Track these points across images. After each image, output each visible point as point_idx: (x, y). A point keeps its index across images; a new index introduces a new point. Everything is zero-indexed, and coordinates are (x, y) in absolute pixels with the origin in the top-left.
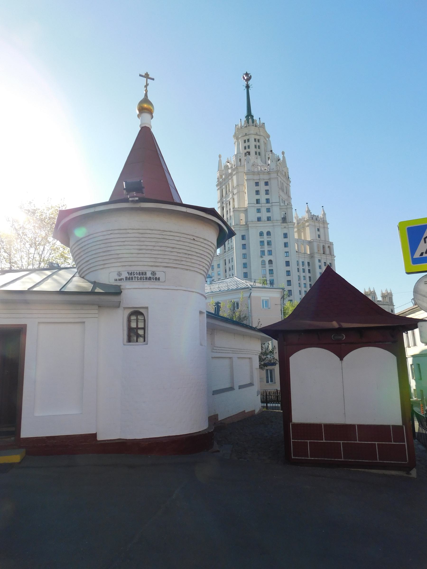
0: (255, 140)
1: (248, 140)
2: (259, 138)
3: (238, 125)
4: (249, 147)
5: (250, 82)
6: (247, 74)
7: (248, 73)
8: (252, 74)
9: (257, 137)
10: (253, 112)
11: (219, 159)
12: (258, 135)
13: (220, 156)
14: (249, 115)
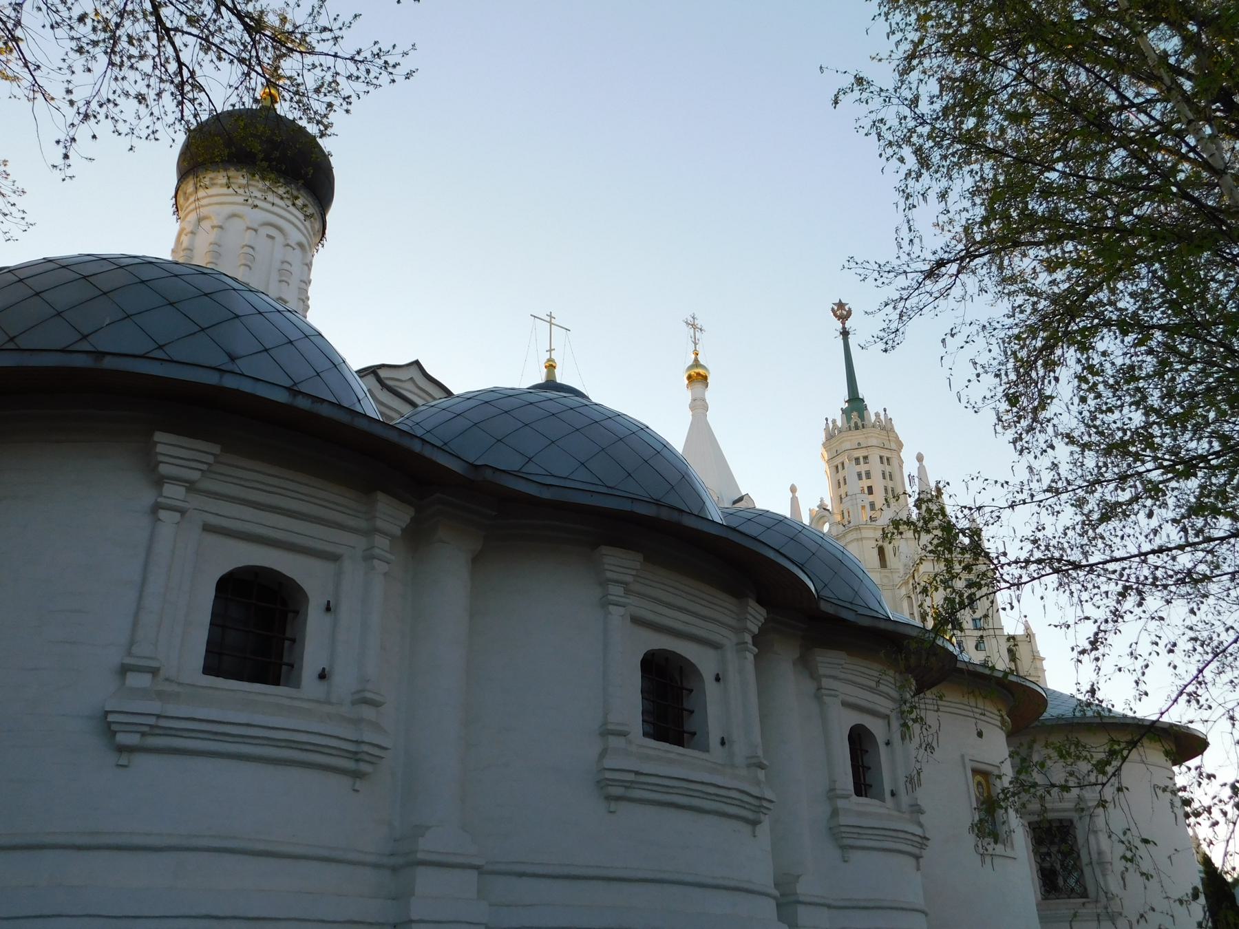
0: (881, 458)
1: (866, 458)
2: (889, 456)
3: (834, 421)
4: (868, 475)
6: (841, 305)
9: (886, 454)
10: (862, 392)
11: (791, 495)
13: (793, 489)
14: (855, 402)
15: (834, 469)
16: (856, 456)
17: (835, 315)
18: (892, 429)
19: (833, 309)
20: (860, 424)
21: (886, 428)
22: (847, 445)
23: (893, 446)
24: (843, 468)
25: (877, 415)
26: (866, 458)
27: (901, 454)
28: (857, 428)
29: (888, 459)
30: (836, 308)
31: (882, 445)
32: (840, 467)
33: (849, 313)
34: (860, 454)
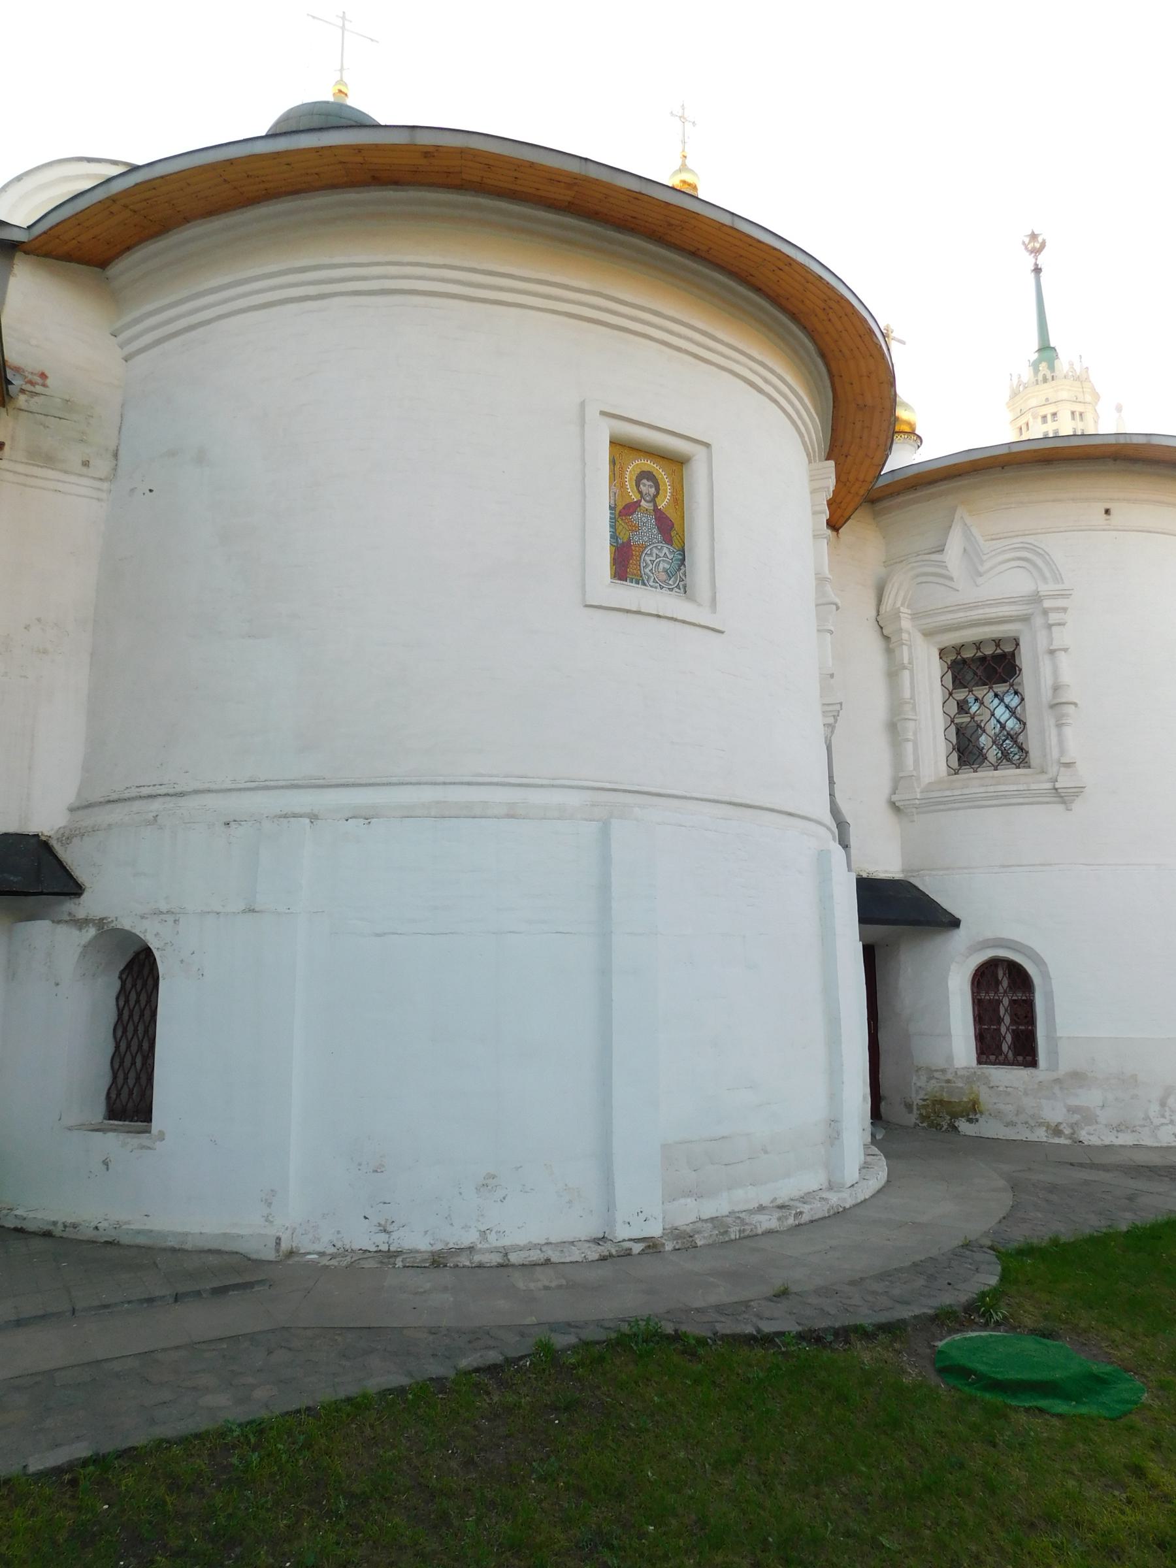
0: (1073, 413)
1: (1054, 415)
5: (1042, 260)
6: (1034, 236)
7: (1036, 233)
8: (1044, 234)
9: (1078, 408)
12: (1080, 402)
14: (1046, 349)
15: (1018, 430)
16: (1043, 413)
17: (1026, 248)
18: (1087, 379)
19: (1024, 243)
20: (1049, 376)
21: (1081, 379)
22: (1033, 402)
23: (1088, 398)
24: (1028, 429)
25: (1072, 365)
26: (1054, 415)
27: (1097, 408)
28: (1045, 380)
29: (1081, 414)
30: (1027, 240)
31: (1075, 399)
32: (1024, 429)
33: (1043, 245)
34: (1048, 410)
